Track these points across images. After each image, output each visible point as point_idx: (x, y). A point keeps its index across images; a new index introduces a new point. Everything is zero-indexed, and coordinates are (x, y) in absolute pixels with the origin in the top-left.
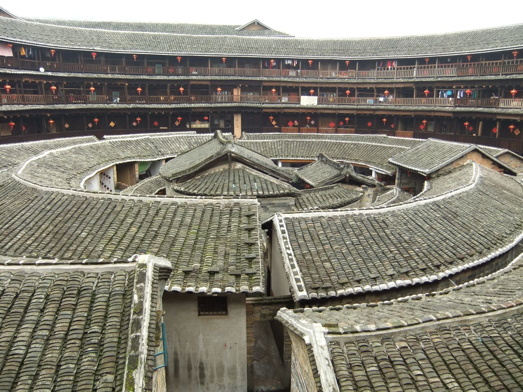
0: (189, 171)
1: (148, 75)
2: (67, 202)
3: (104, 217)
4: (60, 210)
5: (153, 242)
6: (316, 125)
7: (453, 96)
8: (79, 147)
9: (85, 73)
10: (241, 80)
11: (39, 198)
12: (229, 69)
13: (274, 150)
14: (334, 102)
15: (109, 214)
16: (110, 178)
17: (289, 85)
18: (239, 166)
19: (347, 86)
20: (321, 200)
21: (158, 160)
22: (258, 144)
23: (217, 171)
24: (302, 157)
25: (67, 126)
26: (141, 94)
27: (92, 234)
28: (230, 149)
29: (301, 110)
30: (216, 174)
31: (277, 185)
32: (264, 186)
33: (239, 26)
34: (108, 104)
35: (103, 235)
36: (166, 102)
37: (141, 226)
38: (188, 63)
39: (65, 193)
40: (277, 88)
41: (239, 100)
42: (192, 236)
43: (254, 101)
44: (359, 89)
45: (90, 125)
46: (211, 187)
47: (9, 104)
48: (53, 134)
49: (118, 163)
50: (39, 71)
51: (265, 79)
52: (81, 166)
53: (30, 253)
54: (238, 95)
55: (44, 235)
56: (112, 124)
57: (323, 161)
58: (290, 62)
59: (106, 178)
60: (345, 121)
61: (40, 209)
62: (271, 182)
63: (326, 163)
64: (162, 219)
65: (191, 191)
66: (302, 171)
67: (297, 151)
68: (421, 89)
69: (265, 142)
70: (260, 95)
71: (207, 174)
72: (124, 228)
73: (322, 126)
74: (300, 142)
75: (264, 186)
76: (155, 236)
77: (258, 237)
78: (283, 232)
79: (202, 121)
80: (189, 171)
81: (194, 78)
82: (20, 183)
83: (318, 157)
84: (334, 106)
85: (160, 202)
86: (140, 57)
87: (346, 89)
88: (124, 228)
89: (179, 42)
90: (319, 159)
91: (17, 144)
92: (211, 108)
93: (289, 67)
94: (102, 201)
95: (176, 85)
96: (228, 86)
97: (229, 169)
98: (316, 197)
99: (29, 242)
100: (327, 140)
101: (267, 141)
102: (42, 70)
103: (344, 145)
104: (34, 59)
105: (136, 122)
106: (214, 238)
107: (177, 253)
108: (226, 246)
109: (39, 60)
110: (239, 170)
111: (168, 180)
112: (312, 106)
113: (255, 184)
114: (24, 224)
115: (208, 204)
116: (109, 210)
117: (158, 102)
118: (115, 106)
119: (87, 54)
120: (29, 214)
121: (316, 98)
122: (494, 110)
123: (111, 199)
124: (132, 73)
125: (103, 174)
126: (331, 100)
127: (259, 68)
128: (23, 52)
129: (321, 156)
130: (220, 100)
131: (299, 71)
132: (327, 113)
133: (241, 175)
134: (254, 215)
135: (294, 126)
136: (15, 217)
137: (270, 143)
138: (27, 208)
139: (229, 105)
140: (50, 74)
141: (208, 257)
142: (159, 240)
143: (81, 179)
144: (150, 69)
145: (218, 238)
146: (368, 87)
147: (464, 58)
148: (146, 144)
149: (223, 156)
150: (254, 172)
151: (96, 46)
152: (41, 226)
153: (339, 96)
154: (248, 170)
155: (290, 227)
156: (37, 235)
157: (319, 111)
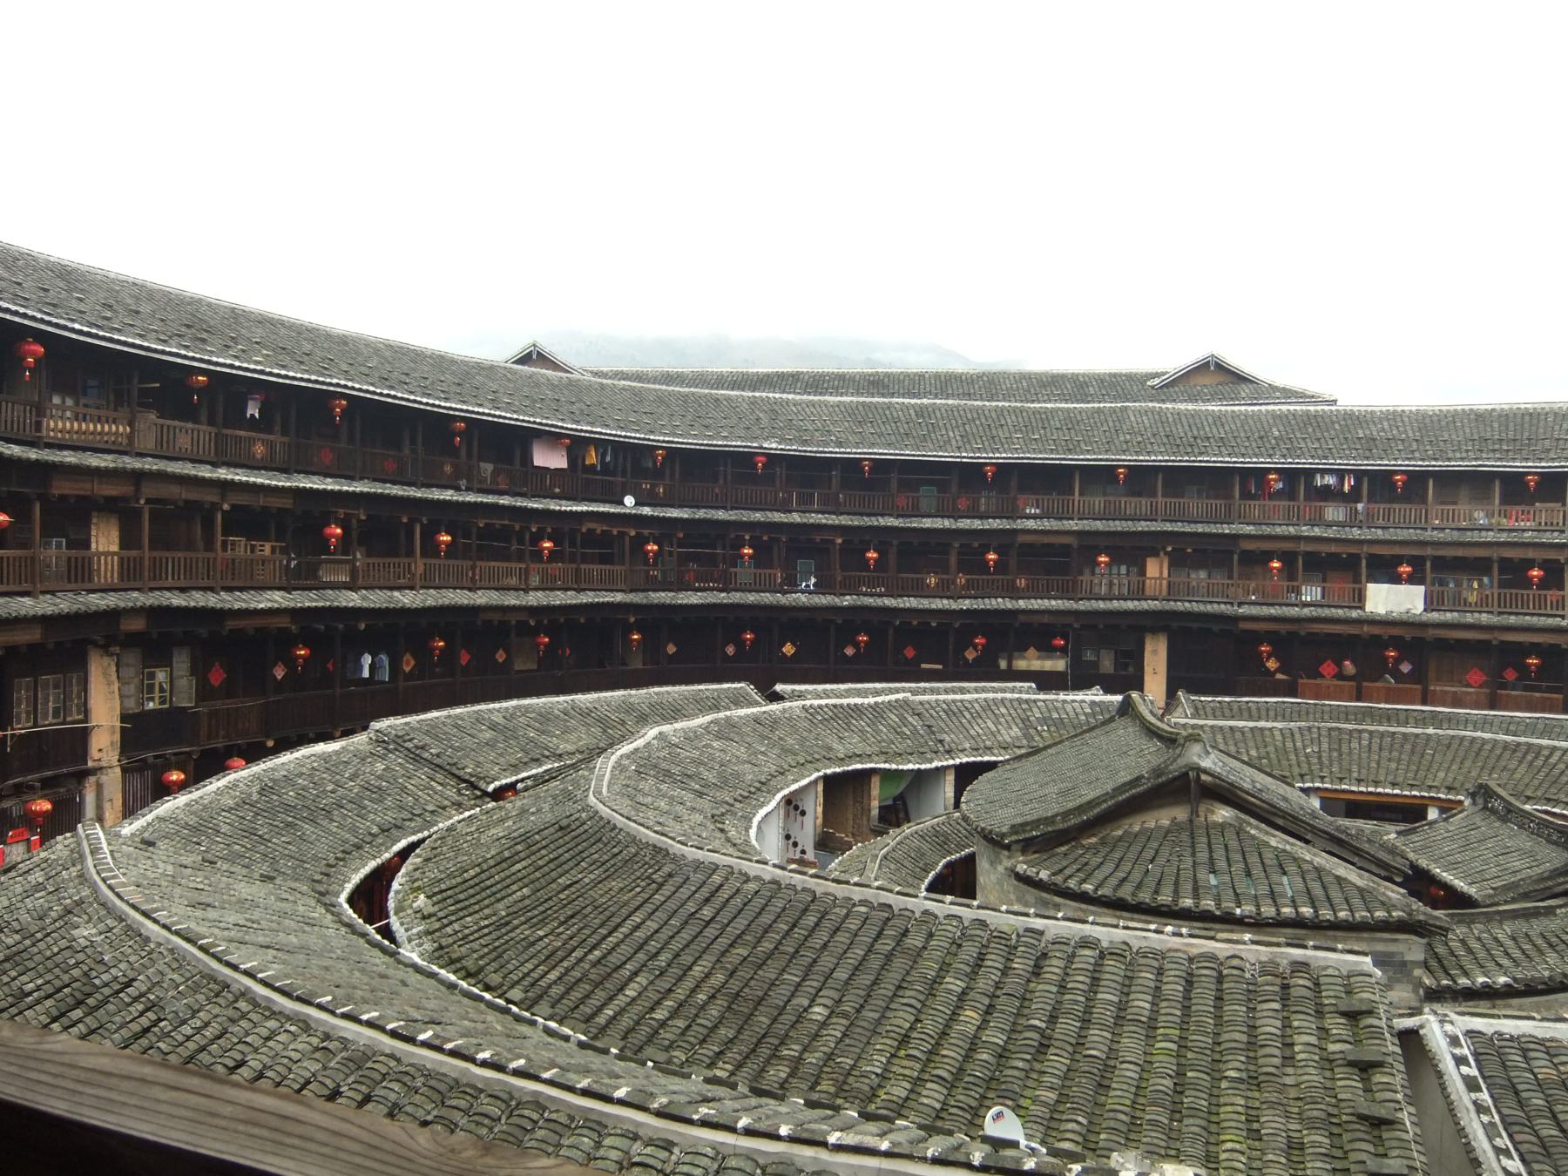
0: (1064, 821)
1: (898, 517)
2: (758, 902)
3: (875, 963)
4: (741, 923)
5: (1037, 1066)
6: (1418, 676)
8: (728, 719)
9: (732, 508)
10: (1172, 533)
11: (678, 879)
12: (1134, 500)
13: (1293, 757)
14: (1483, 604)
15: (889, 957)
16: (803, 813)
17: (1325, 549)
18: (1223, 814)
19: (1530, 554)
20: (1517, 954)
21: (937, 769)
22: (1238, 735)
23: (1152, 825)
24: (1394, 785)
25: (671, 649)
26: (875, 570)
27: (845, 1015)
28: (1196, 759)
29: (1366, 628)
30: (1148, 835)
31: (1361, 890)
32: (1317, 891)
33: (1157, 375)
34: (784, 593)
35: (879, 1022)
36: (943, 591)
37: (990, 1006)
38: (1014, 483)
39: (752, 874)
40: (1288, 558)
41: (1164, 593)
42: (1165, 1063)
43: (1208, 596)
45: (730, 650)
46: (1136, 876)
47: (544, 590)
48: (636, 671)
49: (829, 771)
50: (621, 503)
51: (1249, 529)
52: (737, 775)
53: (667, 1049)
54: (1161, 578)
55: (702, 997)
56: (789, 649)
57: (1493, 811)
58: (1330, 480)
59: (792, 812)
60: (1523, 670)
61: (683, 913)
62: (1338, 878)
63: (1504, 820)
64: (1054, 989)
65: (1072, 883)
66: (1414, 838)
67: (1373, 765)
69: (1262, 729)
70: (1230, 577)
71: (1120, 832)
72: (942, 1005)
73: (1438, 680)
74: (1382, 735)
75: (1317, 891)
76: (1043, 1048)
77: (1399, 1097)
78: (1471, 1085)
79: (1047, 649)
80: (1064, 821)
81: (1031, 524)
82: (615, 827)
83: (1473, 795)
84: (1485, 618)
85: (1042, 933)
86: (880, 465)
87: (1530, 564)
88: (942, 1005)
89: (991, 427)
90: (1474, 803)
91: (561, 698)
92: (1076, 613)
93: (1327, 494)
94: (863, 909)
95: (976, 545)
96: (1132, 550)
97: (1191, 821)
98: (1496, 940)
99: (660, 1014)
100: (1479, 734)
101: (1269, 725)
102: (629, 501)
103: (1546, 752)
104: (613, 474)
105: (856, 645)
106: (1241, 1081)
107: (1123, 1117)
108: (1287, 1115)
109: (624, 474)
110: (1222, 827)
111: (994, 841)
112: (1405, 617)
113: (1285, 879)
114: (641, 956)
115: (1202, 955)
116: (886, 945)
117: (920, 591)
118: (804, 599)
119: (743, 460)
120: (655, 926)
121: (1420, 590)
123: (890, 906)
124: (856, 509)
125: (792, 804)
126: (1473, 598)
127: (1230, 496)
128: (592, 458)
129: (1483, 794)
130: (1105, 593)
131: (1360, 506)
132: (1458, 641)
133: (1234, 844)
134: (1370, 1013)
135: (1341, 676)
136: (615, 929)
137: (1277, 733)
138: (648, 908)
139: (1130, 605)
140: (647, 511)
141: (1229, 1145)
142: (1057, 1061)
143: (748, 819)
144: (902, 501)
145: (1254, 1081)
148: (902, 718)
149: (1175, 779)
150: (1276, 840)
151: (766, 439)
152: (690, 968)
153: (1502, 584)
154: (1255, 829)
155: (1494, 1069)
156: (681, 993)
157: (1431, 632)
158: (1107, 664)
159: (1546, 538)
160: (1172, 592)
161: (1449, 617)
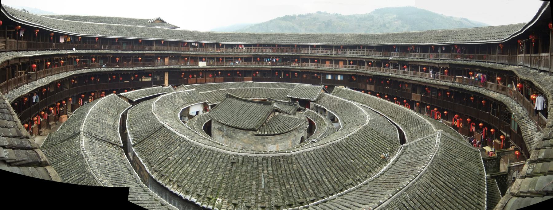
7: (271, 61)
14: (213, 64)
17: (193, 56)
40: (188, 57)
44: (226, 58)
68: (255, 58)
87: (220, 58)
96: (163, 56)
122: (289, 67)
146: (231, 56)
147: (274, 46)
158: (158, 79)
159: (223, 54)
160: (169, 65)
161: (210, 67)
